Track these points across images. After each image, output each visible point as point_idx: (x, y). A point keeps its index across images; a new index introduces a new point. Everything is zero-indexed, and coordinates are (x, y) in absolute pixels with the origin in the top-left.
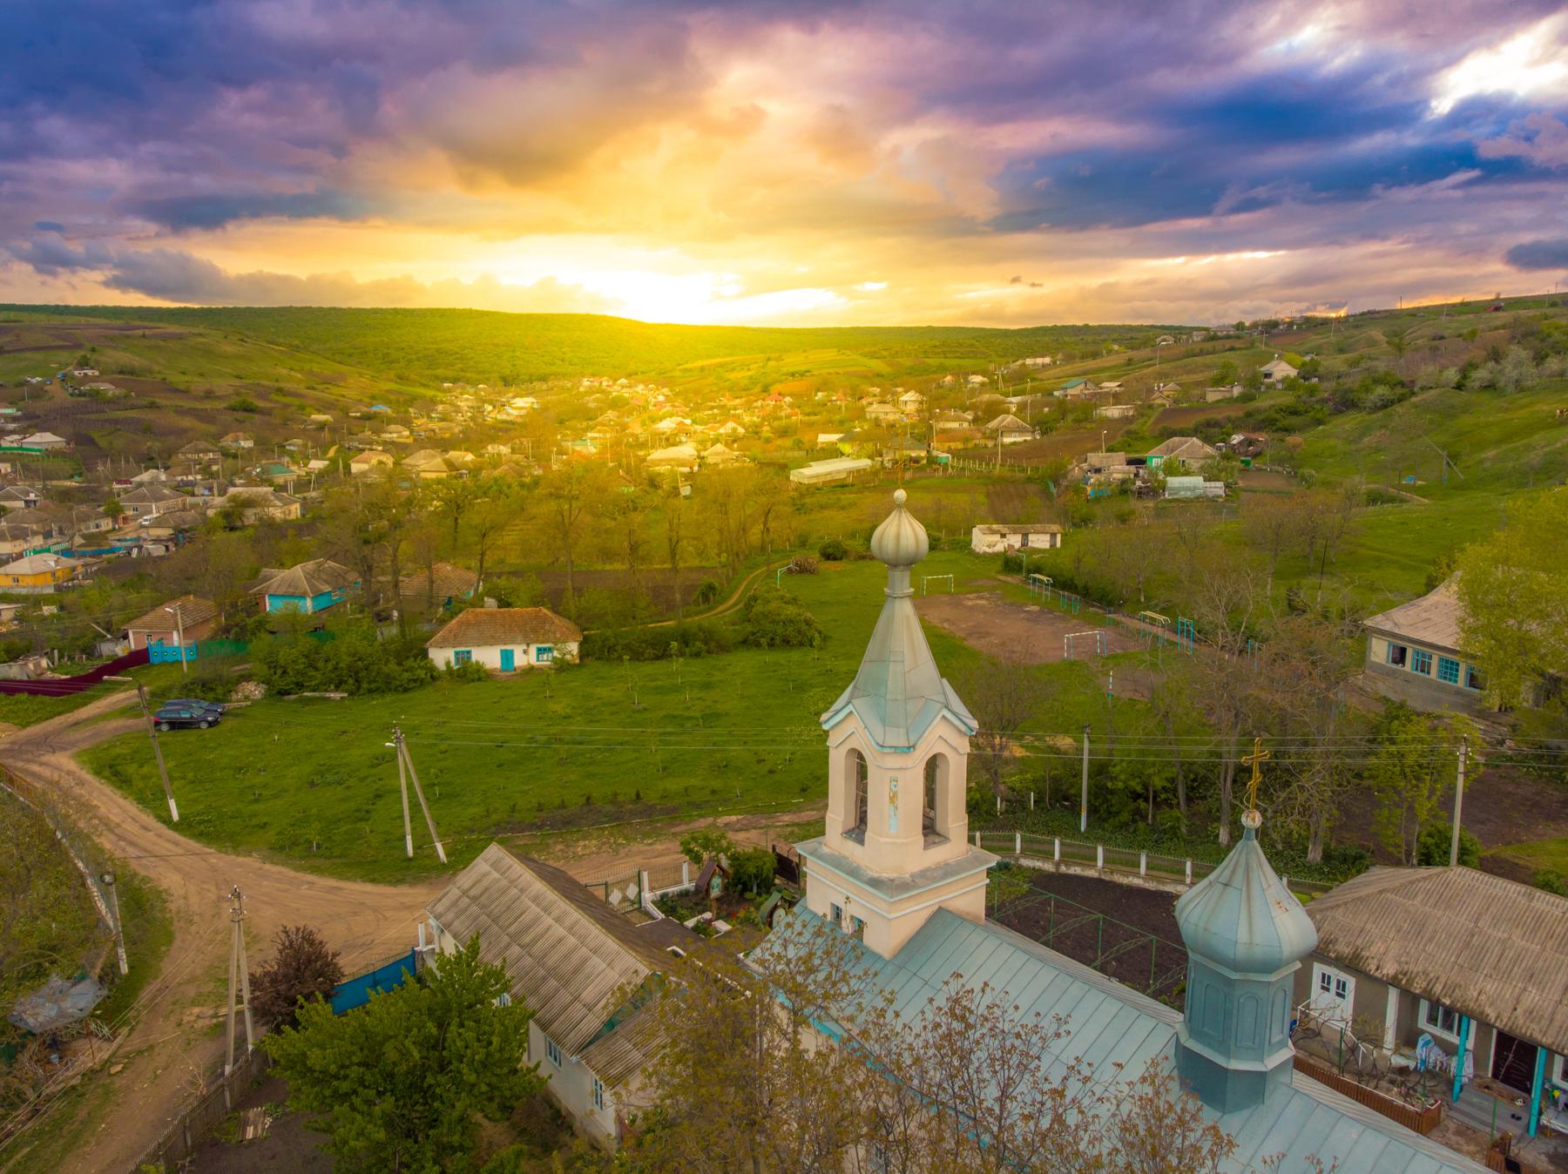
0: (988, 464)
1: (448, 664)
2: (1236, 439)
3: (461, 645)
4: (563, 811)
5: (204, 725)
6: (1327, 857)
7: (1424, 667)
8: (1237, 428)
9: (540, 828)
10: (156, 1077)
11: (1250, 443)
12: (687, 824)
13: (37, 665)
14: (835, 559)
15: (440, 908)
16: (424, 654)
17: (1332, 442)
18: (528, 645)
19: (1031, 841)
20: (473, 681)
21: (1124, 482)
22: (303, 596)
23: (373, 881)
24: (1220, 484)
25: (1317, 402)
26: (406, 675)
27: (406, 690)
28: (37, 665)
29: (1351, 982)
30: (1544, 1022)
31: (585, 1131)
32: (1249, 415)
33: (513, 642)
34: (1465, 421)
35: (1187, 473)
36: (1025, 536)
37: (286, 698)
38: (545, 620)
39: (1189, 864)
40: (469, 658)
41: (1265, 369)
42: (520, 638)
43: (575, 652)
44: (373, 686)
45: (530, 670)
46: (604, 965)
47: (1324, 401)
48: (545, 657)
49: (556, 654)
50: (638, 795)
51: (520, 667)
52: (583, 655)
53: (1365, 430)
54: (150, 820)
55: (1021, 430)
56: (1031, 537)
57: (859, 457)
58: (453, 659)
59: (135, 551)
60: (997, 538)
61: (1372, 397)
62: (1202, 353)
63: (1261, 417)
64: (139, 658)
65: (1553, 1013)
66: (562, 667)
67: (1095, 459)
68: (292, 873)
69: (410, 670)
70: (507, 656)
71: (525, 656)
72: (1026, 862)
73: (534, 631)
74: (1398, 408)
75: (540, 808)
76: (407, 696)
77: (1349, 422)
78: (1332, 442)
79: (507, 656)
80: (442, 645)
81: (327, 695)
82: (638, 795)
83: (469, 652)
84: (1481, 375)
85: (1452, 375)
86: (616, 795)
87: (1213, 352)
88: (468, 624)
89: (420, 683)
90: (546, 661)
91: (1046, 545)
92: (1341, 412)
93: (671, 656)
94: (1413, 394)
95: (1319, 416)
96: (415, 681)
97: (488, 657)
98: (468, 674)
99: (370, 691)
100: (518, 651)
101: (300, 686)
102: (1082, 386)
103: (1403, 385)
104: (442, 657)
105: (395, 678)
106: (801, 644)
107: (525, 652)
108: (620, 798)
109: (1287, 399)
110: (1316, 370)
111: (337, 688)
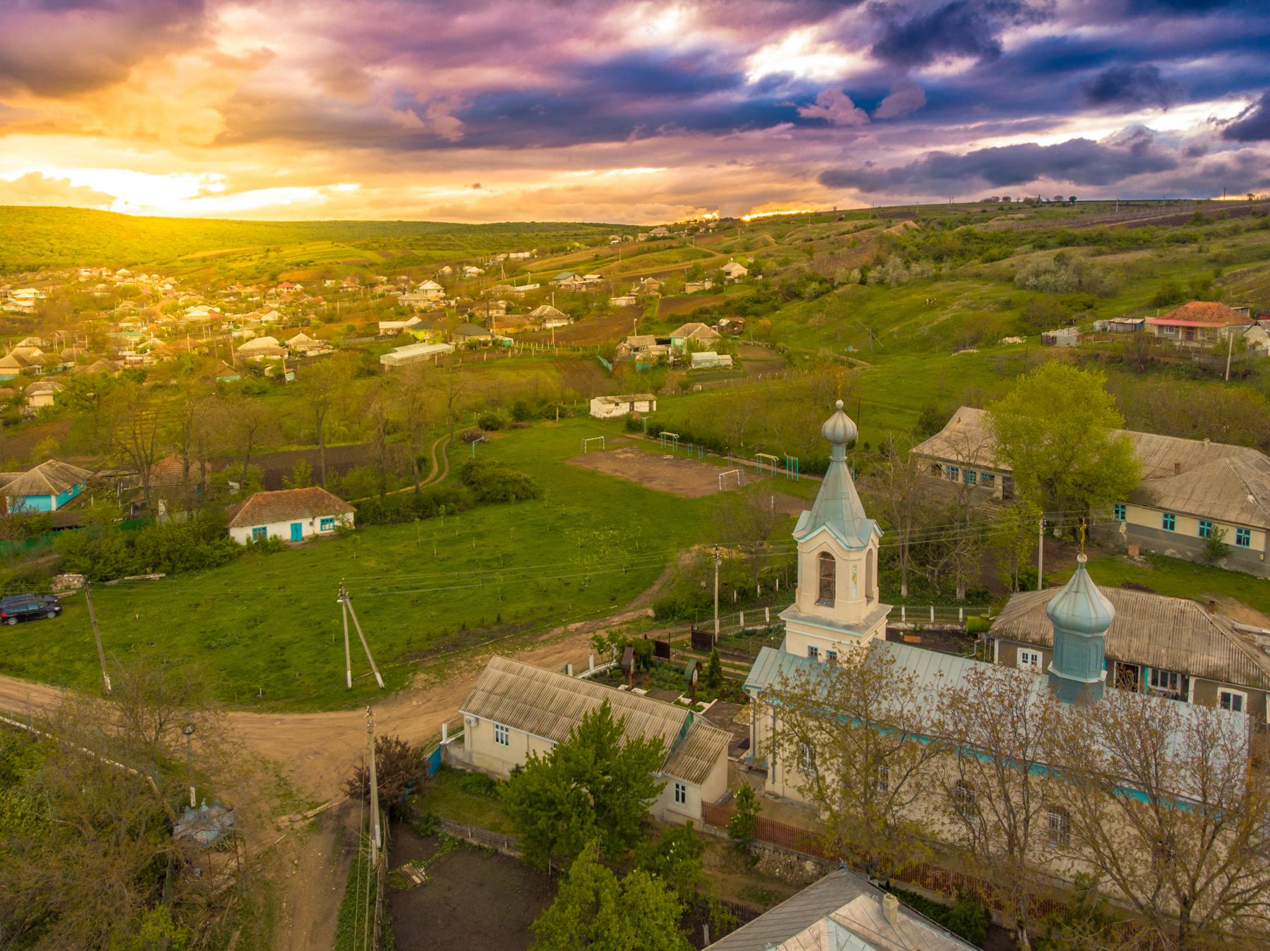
0: (545, 346)
1: (248, 539)
2: (724, 322)
3: (258, 523)
4: (447, 638)
5: (51, 615)
6: (968, 595)
7: (954, 476)
8: (722, 315)
9: (438, 651)
10: (297, 865)
11: (732, 325)
12: (547, 633)
14: (492, 429)
16: (226, 532)
17: (789, 323)
18: (314, 518)
19: (750, 614)
20: (274, 551)
21: (661, 357)
22: (48, 494)
23: (332, 710)
24: (728, 357)
25: (772, 294)
26: (218, 552)
27: (218, 565)
29: (1040, 655)
30: (1145, 655)
31: (666, 822)
32: (728, 304)
33: (302, 517)
34: (871, 307)
35: (702, 350)
36: (632, 404)
37: (108, 583)
38: (322, 497)
39: (903, 609)
40: (265, 533)
41: (725, 268)
42: (307, 513)
43: (352, 520)
44: (188, 565)
45: (316, 539)
46: (648, 715)
47: (775, 293)
48: (327, 527)
49: (337, 523)
50: (499, 619)
51: (307, 537)
52: (359, 521)
53: (810, 313)
55: (559, 318)
56: (636, 404)
57: (434, 343)
58: (251, 535)
60: (613, 406)
61: (808, 290)
62: (649, 251)
63: (736, 306)
65: (1148, 650)
66: (342, 533)
67: (633, 340)
68: (257, 716)
69: (219, 547)
70: (296, 529)
71: (311, 527)
73: (316, 506)
74: (827, 298)
75: (429, 638)
76: (223, 570)
77: (796, 307)
78: (789, 323)
79: (296, 529)
80: (242, 524)
81: (147, 577)
82: (499, 619)
83: (265, 529)
84: (873, 274)
85: (856, 274)
86: (483, 620)
87: (658, 250)
88: (260, 506)
89: (230, 558)
90: (329, 529)
91: (647, 409)
92: (788, 301)
93: (439, 515)
94: (834, 288)
95: (776, 304)
96: (225, 556)
97: (280, 530)
98: (264, 547)
99: (186, 569)
100: (305, 523)
101: (120, 572)
103: (825, 281)
104: (241, 535)
105: (208, 556)
106: (527, 498)
107: (311, 524)
108: (486, 623)
109: (750, 292)
110: (760, 270)
111: (153, 572)
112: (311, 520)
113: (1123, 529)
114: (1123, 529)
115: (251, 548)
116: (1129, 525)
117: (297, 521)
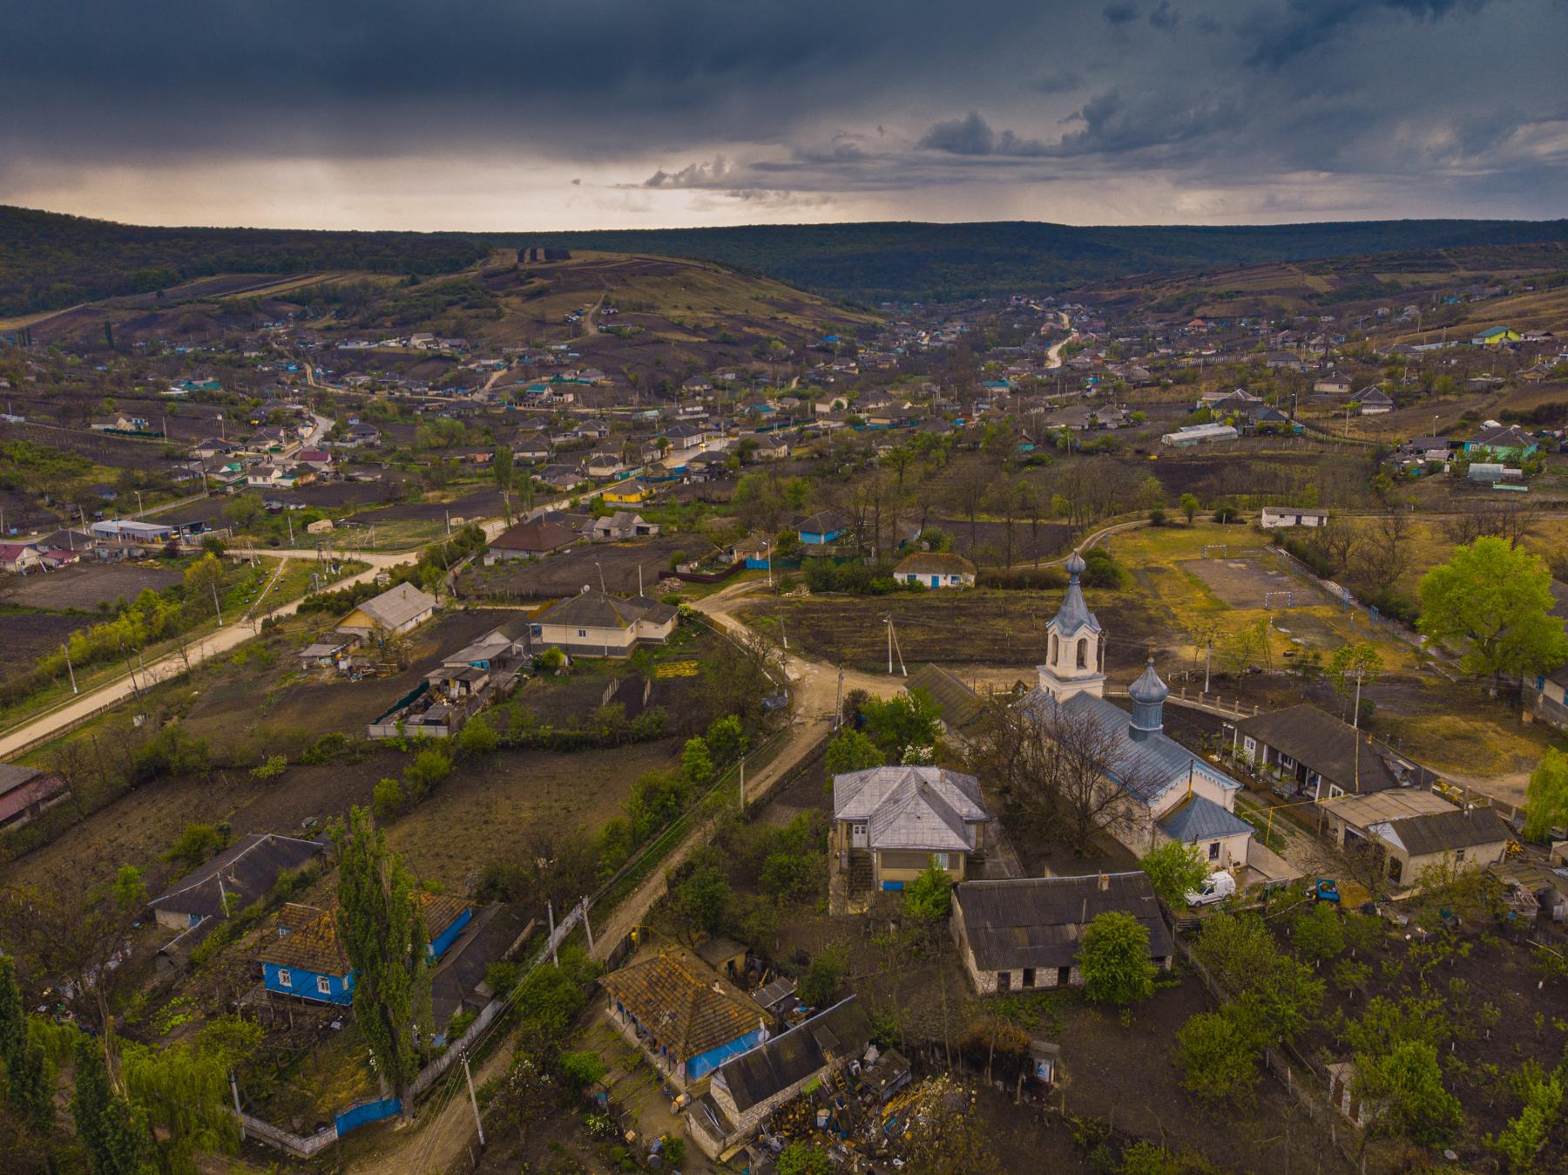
52: (978, 583)
70: (935, 580)
79: (935, 580)
97: (926, 580)
98: (914, 587)
100: (941, 578)
102: (1503, 335)
113: (1540, 700)
114: (1540, 700)
116: (1545, 696)
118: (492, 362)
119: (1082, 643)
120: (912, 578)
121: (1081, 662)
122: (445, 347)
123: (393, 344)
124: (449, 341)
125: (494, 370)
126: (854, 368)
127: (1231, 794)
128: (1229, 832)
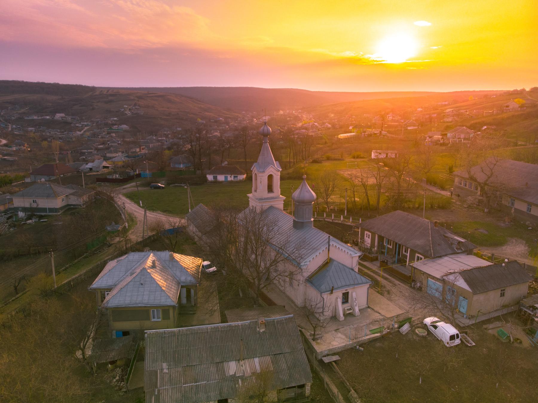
13: (116, 176)
15: (188, 215)
22: (180, 163)
28: (116, 176)
33: (227, 174)
45: (231, 182)
48: (236, 178)
54: (137, 206)
55: (414, 126)
59: (144, 156)
64: (139, 176)
70: (226, 178)
72: (326, 220)
79: (226, 178)
80: (210, 174)
81: (181, 185)
83: (217, 176)
98: (216, 182)
100: (229, 176)
104: (210, 178)
107: (231, 177)
112: (230, 175)
113: (513, 211)
114: (513, 211)
115: (211, 182)
116: (515, 209)
117: (226, 175)
118: (85, 123)
119: (270, 177)
120: (215, 178)
121: (270, 189)
122: (69, 119)
123: (48, 117)
124: (71, 117)
125: (86, 126)
126: (228, 128)
127: (356, 260)
128: (356, 284)
